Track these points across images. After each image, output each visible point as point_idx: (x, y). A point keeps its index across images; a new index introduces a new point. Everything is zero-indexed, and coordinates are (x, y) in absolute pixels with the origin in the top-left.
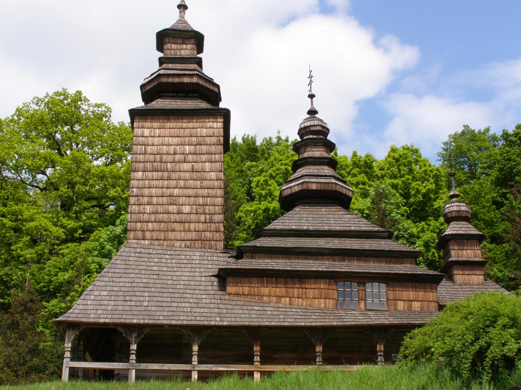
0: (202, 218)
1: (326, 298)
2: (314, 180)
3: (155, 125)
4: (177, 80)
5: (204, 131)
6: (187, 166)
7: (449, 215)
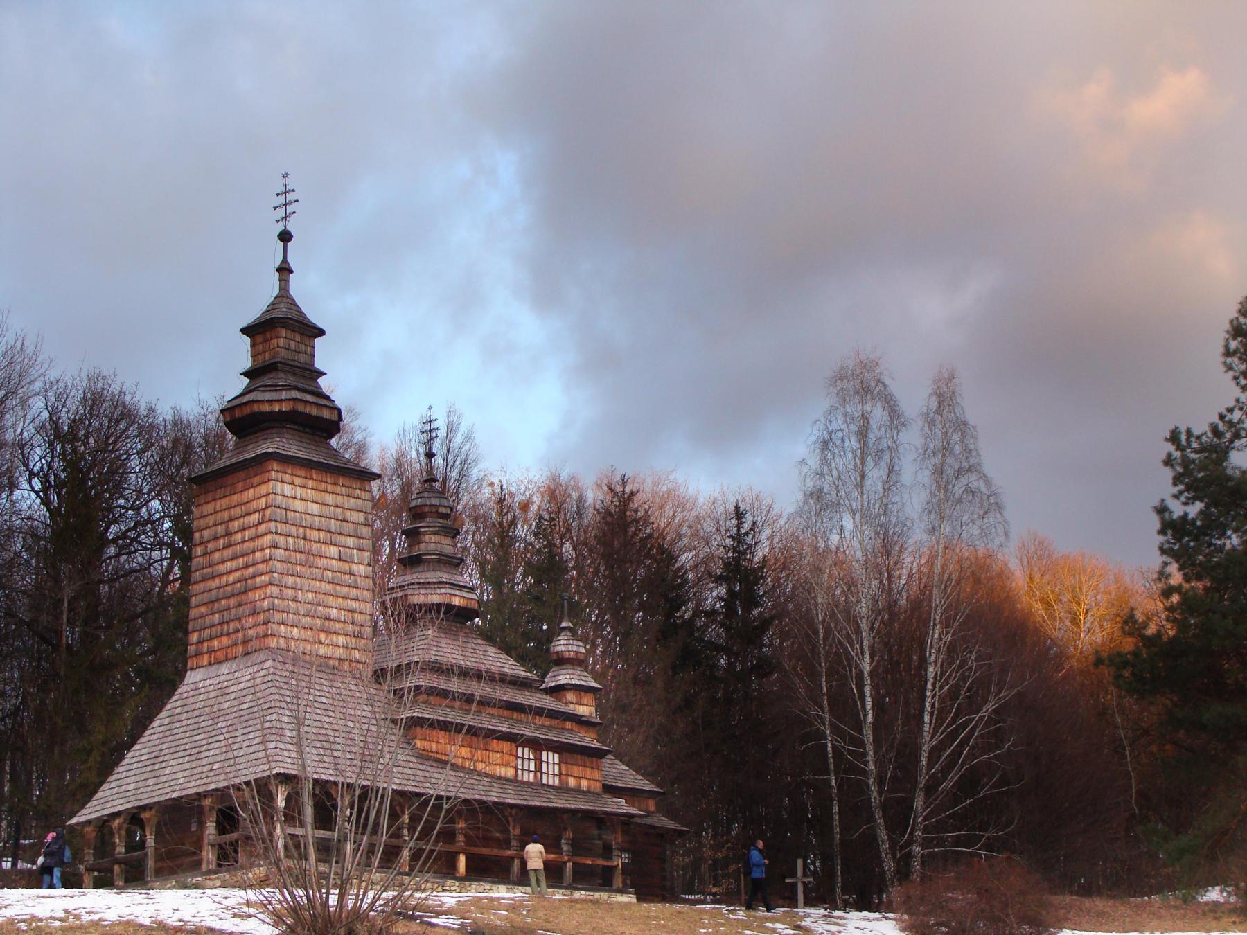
0: (350, 628)
1: (507, 765)
2: (457, 593)
3: (297, 480)
4: (314, 412)
5: (352, 500)
6: (333, 551)
7: (566, 655)
